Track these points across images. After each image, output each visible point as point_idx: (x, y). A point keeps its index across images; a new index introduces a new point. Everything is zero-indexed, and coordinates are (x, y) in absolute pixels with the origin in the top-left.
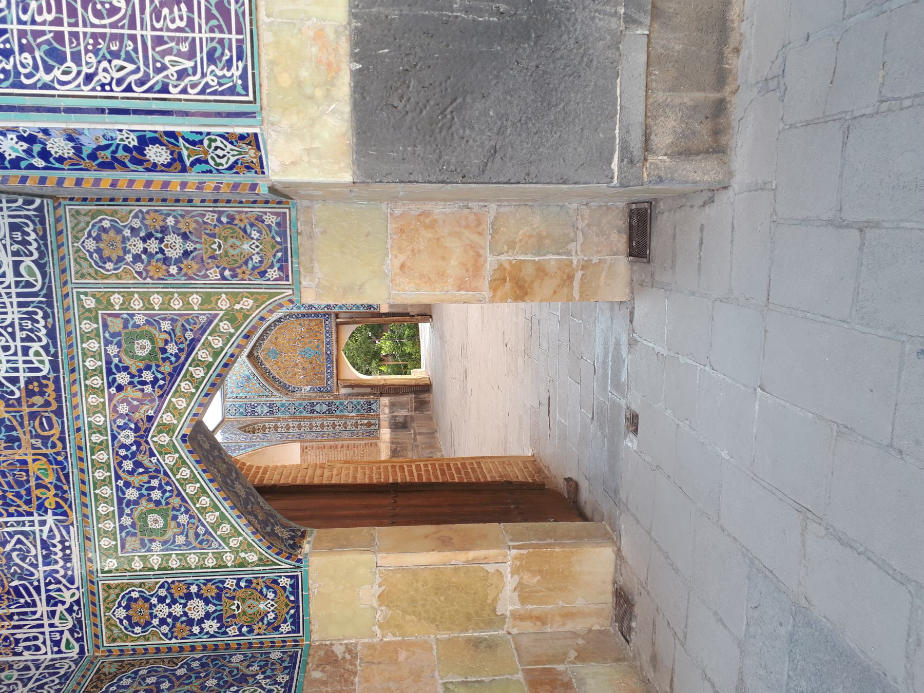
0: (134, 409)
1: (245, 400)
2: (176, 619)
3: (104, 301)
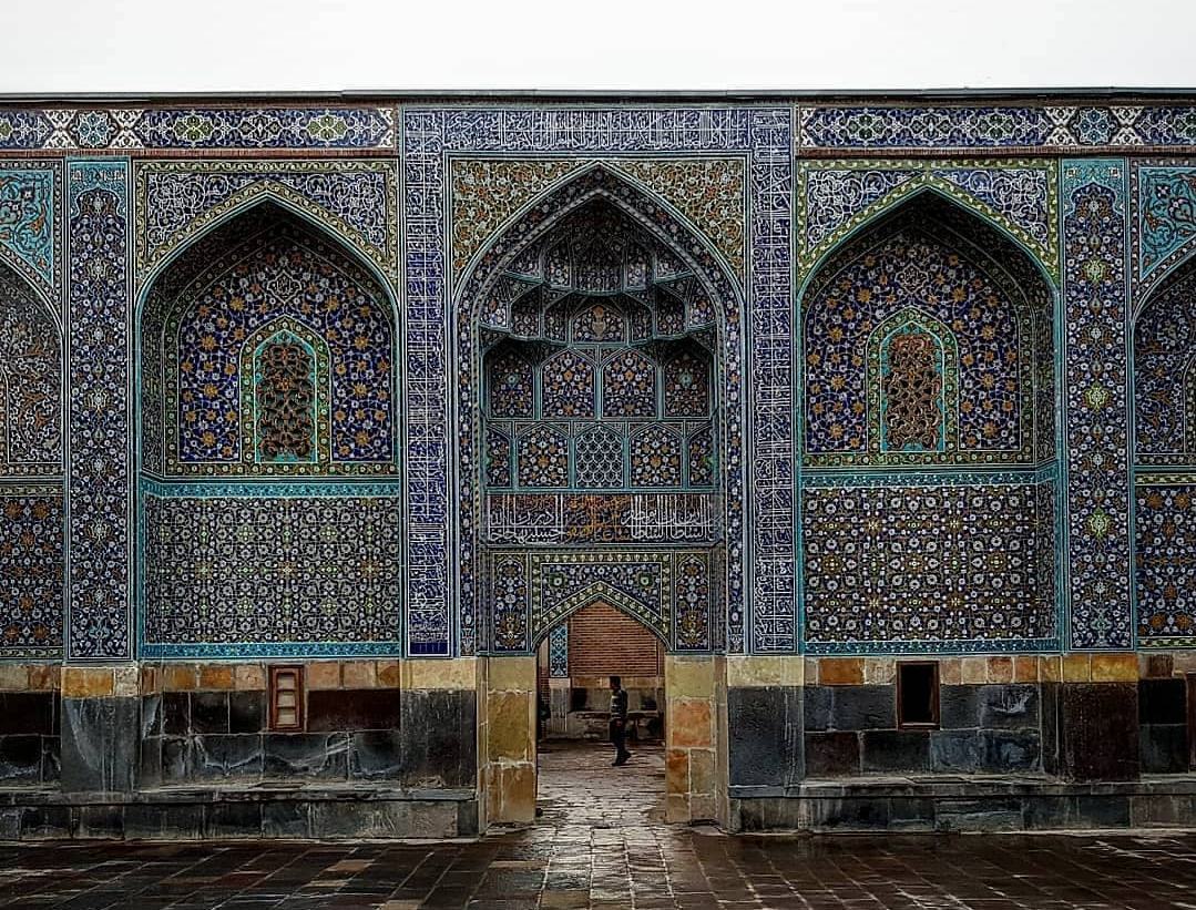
0: (615, 575)
2: (506, 589)
3: (666, 564)
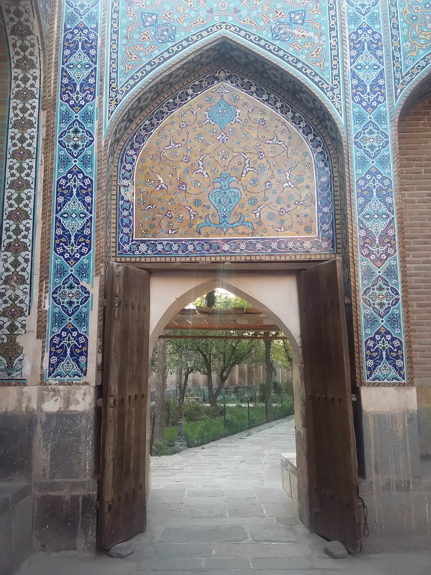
1: (108, 30)
